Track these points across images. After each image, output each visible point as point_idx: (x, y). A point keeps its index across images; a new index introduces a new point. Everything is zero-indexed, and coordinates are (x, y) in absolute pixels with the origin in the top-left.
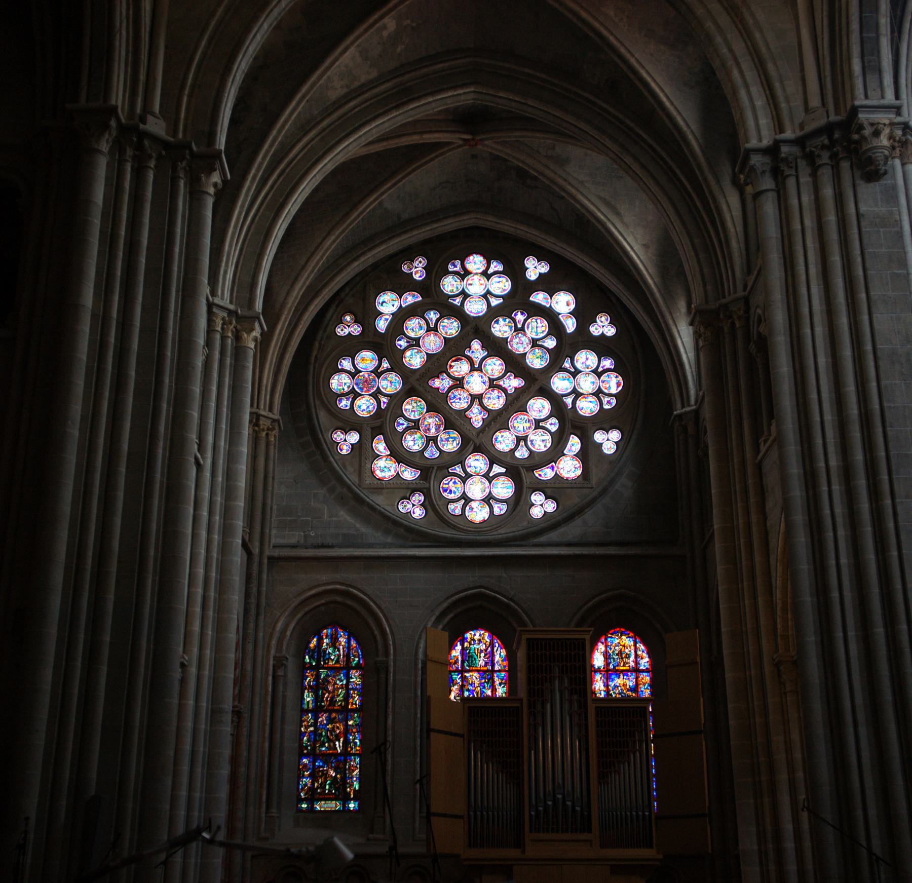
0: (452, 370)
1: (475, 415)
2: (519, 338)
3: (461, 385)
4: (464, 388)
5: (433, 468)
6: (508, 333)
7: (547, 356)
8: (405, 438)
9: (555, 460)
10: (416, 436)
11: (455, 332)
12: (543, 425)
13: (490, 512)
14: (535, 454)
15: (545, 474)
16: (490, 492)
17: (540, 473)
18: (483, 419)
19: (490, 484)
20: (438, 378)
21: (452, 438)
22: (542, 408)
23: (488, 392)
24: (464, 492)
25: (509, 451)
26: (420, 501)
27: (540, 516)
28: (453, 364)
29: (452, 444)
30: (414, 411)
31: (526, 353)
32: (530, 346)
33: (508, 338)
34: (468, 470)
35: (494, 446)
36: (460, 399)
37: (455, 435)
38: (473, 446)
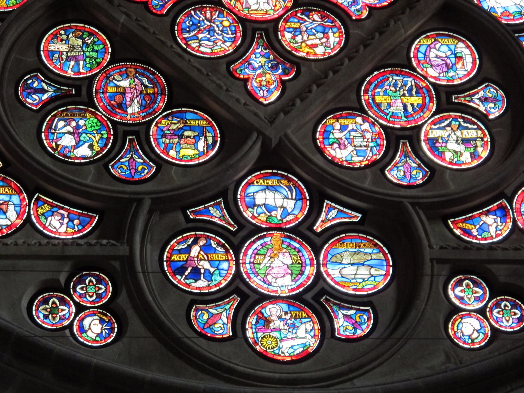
1: (259, 72)
4: (224, 6)
5: (140, 202)
8: (49, 126)
9: (508, 192)
10: (81, 122)
12: (462, 100)
13: (322, 329)
14: (448, 173)
15: (481, 230)
16: (319, 275)
17: (467, 226)
18: (283, 83)
19: (317, 251)
21: (191, 129)
22: (453, 60)
23: (295, 15)
24: (238, 274)
25: (367, 166)
26: (99, 297)
27: (480, 341)
30: (76, 59)
34: (248, 214)
35: (321, 151)
36: (210, 30)
37: (203, 123)
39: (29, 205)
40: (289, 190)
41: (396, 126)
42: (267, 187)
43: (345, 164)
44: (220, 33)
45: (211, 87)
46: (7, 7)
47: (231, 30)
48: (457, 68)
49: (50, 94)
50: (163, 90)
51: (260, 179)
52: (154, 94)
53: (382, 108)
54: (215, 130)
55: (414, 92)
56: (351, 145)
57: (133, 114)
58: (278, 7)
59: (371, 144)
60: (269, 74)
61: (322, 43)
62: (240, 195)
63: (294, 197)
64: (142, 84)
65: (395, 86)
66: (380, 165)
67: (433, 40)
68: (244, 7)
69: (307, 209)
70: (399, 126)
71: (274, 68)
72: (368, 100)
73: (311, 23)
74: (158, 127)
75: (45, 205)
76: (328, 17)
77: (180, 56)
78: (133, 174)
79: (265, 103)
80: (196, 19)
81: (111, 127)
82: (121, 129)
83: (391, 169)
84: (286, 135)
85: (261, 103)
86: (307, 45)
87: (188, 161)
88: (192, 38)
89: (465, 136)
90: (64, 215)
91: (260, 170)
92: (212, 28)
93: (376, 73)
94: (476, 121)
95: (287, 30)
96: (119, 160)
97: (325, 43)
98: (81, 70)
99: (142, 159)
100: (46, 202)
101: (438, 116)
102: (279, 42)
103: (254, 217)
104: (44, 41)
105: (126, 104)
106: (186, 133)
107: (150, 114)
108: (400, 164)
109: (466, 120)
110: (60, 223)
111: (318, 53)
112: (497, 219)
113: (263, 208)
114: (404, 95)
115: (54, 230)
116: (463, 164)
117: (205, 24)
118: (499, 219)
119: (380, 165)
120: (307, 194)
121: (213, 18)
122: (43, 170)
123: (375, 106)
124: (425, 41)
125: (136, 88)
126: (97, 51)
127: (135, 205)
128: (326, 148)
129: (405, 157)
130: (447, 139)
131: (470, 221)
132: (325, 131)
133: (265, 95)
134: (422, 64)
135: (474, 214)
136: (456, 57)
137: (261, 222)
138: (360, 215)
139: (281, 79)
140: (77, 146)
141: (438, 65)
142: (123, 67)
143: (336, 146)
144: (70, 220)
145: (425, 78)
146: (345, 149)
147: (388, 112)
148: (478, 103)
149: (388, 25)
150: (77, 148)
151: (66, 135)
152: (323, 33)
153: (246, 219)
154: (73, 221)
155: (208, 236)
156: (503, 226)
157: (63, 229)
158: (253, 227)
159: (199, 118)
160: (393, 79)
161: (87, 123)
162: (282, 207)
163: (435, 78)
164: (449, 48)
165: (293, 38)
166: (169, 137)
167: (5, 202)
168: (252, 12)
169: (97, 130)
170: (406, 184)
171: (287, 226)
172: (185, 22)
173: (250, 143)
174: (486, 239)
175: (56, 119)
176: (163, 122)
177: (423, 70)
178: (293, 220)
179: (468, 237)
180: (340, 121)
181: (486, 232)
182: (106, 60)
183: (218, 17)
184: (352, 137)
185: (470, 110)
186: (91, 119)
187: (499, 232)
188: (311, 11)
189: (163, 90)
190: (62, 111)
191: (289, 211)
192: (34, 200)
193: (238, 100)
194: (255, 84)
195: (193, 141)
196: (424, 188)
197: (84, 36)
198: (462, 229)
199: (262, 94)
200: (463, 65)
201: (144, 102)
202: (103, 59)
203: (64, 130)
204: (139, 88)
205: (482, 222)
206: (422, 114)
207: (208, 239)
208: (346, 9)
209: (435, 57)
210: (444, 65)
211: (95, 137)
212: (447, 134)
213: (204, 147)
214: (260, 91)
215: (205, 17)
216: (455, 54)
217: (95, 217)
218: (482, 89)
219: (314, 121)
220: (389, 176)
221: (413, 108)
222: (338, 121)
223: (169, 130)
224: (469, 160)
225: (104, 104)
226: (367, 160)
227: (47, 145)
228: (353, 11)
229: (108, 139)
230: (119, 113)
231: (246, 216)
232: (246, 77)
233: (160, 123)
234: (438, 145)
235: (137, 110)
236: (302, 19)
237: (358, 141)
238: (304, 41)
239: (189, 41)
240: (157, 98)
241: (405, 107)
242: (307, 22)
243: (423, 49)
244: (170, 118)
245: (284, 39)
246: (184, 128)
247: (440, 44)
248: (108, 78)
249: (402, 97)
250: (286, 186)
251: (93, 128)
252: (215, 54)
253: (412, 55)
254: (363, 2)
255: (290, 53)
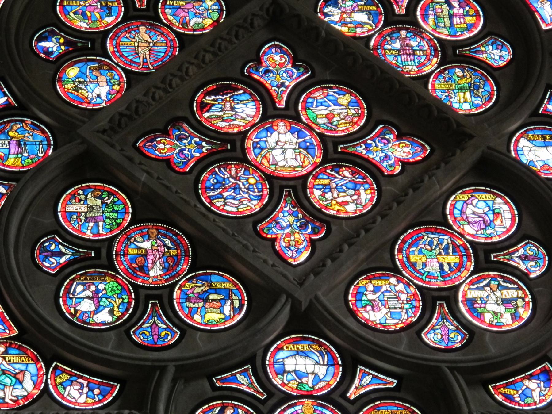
0: (206, 115)
1: (287, 231)
2: (403, 40)
3: (238, 153)
4: (249, 163)
5: (163, 370)
6: (367, 27)
7: (490, 86)
8: (67, 291)
10: (101, 286)
11: (209, 22)
15: (524, 395)
17: (508, 391)
18: (312, 242)
20: (166, 133)
21: (216, 292)
22: (491, 217)
23: (324, 172)
25: (402, 329)
28: (209, 99)
29: (221, 308)
30: (95, 220)
31: (428, 76)
32: (435, 60)
33: (369, 38)
34: (277, 381)
35: (353, 314)
36: (236, 188)
37: (229, 285)
38: (288, 308)
39: (47, 374)
40: (321, 355)
41: (432, 286)
42: (298, 353)
43: (379, 327)
44: (246, 191)
45: (237, 248)
46: (23, 167)
47: (257, 188)
48: (495, 225)
49: (68, 256)
50: (187, 251)
51: (290, 343)
52: (177, 255)
53: (418, 268)
54: (241, 293)
55: (450, 251)
56: (385, 307)
57: (156, 277)
58: (306, 163)
59: (407, 306)
60: (298, 233)
61: (353, 201)
62: (269, 361)
63: (326, 363)
64: (165, 245)
65: (431, 243)
66: (417, 328)
67: (470, 196)
68: (270, 163)
69: (340, 376)
70: (436, 287)
71: (303, 227)
72: (403, 259)
73: (342, 179)
74: (182, 290)
75: (64, 374)
76: (359, 173)
77: (204, 215)
78: (156, 340)
79: (294, 263)
80: (221, 177)
81: (132, 291)
82: (143, 293)
83: (428, 332)
84: (317, 298)
85: (290, 264)
86: (337, 203)
87: (214, 326)
88: (216, 197)
89: (505, 296)
90: (83, 384)
91: (289, 335)
92: (237, 186)
93: (410, 231)
94: (516, 280)
95: (317, 187)
96: (141, 326)
97: (356, 200)
98: (101, 232)
99: (166, 324)
100: (64, 371)
101: (476, 276)
102: (308, 199)
103: (284, 384)
104: (61, 201)
105: (148, 266)
106: (211, 297)
107: (174, 277)
108: (437, 327)
109: (506, 280)
110: (79, 392)
111: (349, 211)
112: (540, 383)
113: (293, 374)
114: (440, 254)
115: (73, 400)
116: (504, 325)
117: (230, 182)
118: (542, 383)
119: (417, 328)
120: (339, 359)
121: (239, 175)
122: (62, 338)
123: (410, 266)
124: (461, 197)
125: (158, 250)
126: (117, 212)
127: (158, 373)
128: (359, 311)
129: (443, 319)
130: (486, 300)
131: (512, 386)
132: (357, 293)
133: (294, 255)
134: (459, 221)
135: (516, 378)
136: (494, 213)
137: (291, 389)
138: (396, 381)
139: (310, 239)
140: (97, 311)
141: (475, 223)
142: (144, 227)
143: (369, 308)
144: (90, 390)
145: (462, 235)
146: (379, 311)
147: (423, 272)
148: (518, 261)
149: (422, 181)
150: (97, 313)
151: (85, 300)
152: (354, 189)
153: (275, 386)
154: (92, 391)
155: (235, 405)
156: (547, 391)
157: (82, 399)
158: (283, 395)
159: (225, 280)
160: (428, 237)
161: (107, 287)
162: (313, 373)
163: (472, 235)
164: (487, 204)
165: (323, 195)
166: (193, 301)
167: (22, 371)
168: (279, 169)
169: (118, 294)
170: (444, 347)
171: (319, 394)
172: (209, 180)
173: (279, 306)
174: (529, 405)
175: (75, 283)
176: (187, 285)
177: (460, 227)
178: (325, 387)
179: (510, 403)
180: (373, 282)
181: (530, 397)
182: (126, 221)
183: (244, 174)
184: (386, 299)
185: (509, 269)
186: (112, 283)
187: (543, 398)
188: (341, 167)
189: (187, 251)
190: (81, 275)
191: (321, 377)
192: (51, 369)
193: (265, 261)
194: (283, 244)
195: (219, 304)
196: (463, 351)
197: (104, 196)
198: (503, 394)
199: (291, 255)
200: (502, 222)
201: (167, 265)
202: (123, 219)
203: (82, 295)
204: (162, 249)
205: (525, 387)
206: (459, 274)
207: (235, 409)
208: (378, 164)
209: (472, 214)
210: (482, 222)
211: (115, 302)
212: (487, 294)
213: (230, 311)
214: (288, 251)
215: (230, 174)
216: (493, 210)
217: (116, 386)
218: (522, 247)
219: (347, 281)
220: (426, 340)
221: (450, 268)
222: (371, 282)
223: (193, 293)
224: (510, 321)
225: (125, 267)
226: (402, 323)
227: (65, 311)
228: (385, 166)
229: (129, 303)
230: (140, 276)
231: (276, 383)
232: (274, 236)
233: (184, 286)
234: (476, 306)
235: (160, 273)
236: (332, 175)
237: (392, 303)
238: (334, 199)
239: (214, 200)
240: (181, 260)
241: (441, 266)
242: (338, 178)
243: (459, 205)
244: (194, 281)
245: (313, 196)
246: (209, 291)
247: (477, 200)
248: (129, 240)
249: (438, 256)
250: (317, 351)
251: (114, 293)
252: (241, 212)
253: (448, 212)
254: (395, 157)
255: (319, 211)
